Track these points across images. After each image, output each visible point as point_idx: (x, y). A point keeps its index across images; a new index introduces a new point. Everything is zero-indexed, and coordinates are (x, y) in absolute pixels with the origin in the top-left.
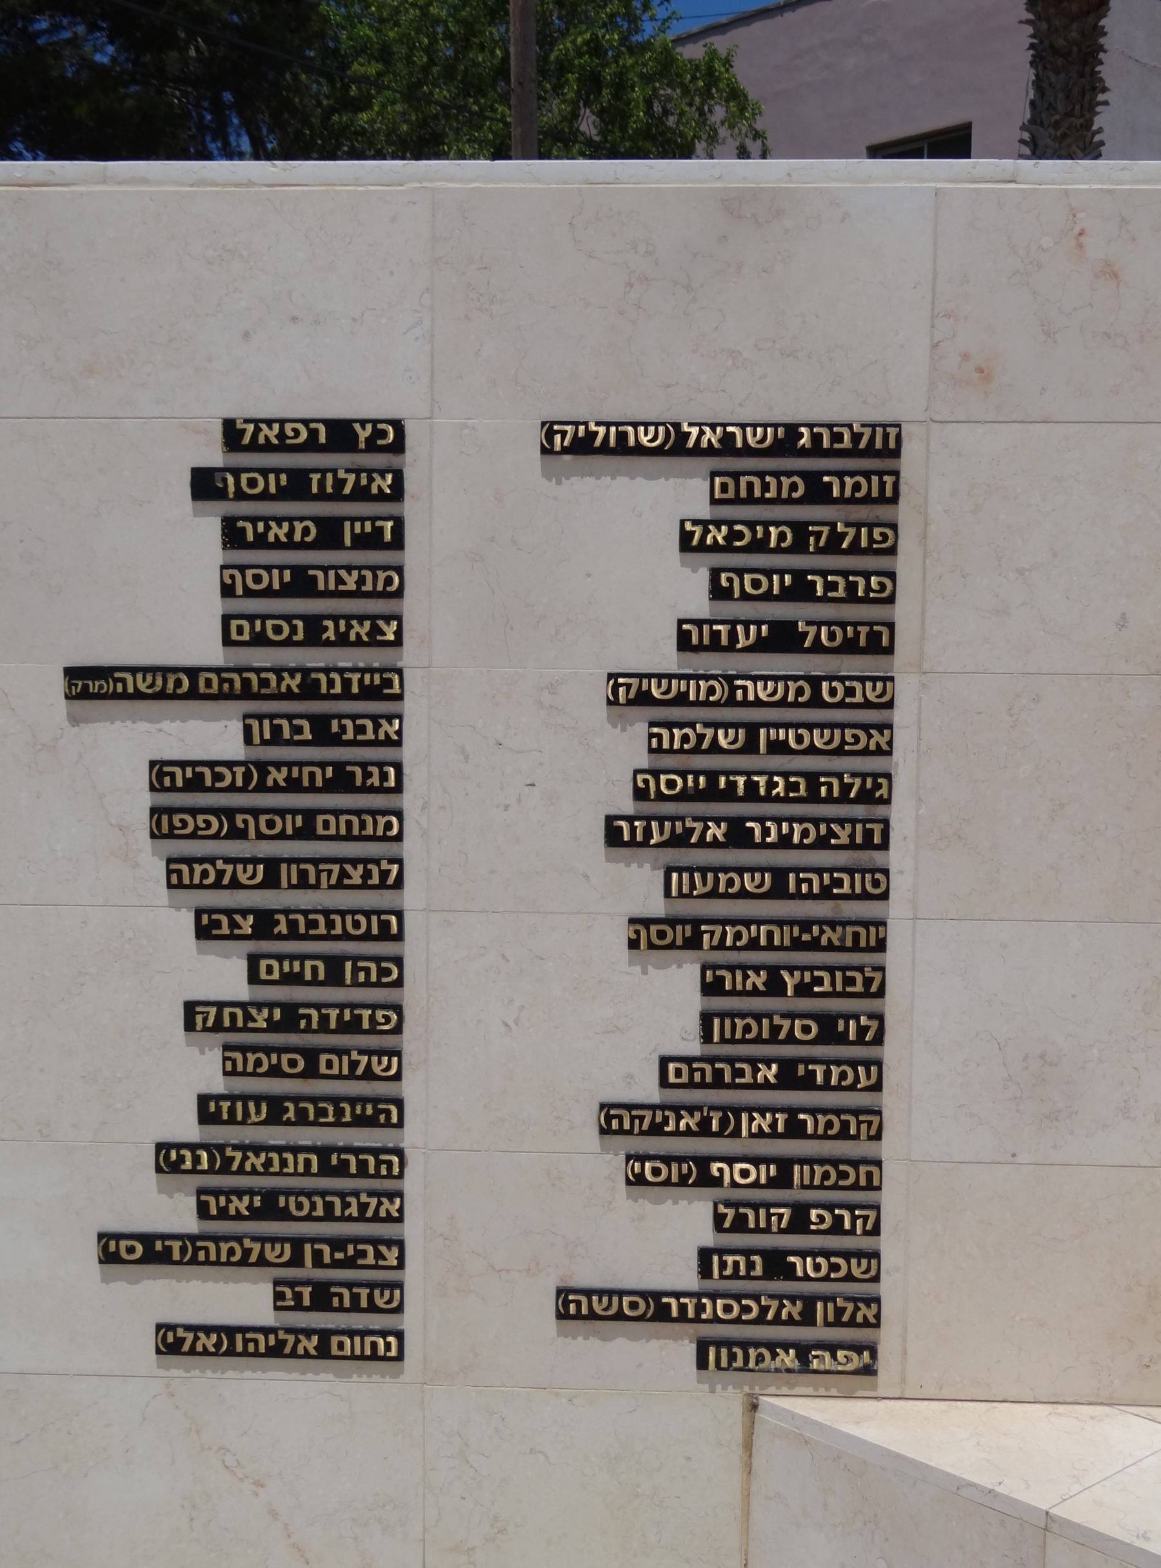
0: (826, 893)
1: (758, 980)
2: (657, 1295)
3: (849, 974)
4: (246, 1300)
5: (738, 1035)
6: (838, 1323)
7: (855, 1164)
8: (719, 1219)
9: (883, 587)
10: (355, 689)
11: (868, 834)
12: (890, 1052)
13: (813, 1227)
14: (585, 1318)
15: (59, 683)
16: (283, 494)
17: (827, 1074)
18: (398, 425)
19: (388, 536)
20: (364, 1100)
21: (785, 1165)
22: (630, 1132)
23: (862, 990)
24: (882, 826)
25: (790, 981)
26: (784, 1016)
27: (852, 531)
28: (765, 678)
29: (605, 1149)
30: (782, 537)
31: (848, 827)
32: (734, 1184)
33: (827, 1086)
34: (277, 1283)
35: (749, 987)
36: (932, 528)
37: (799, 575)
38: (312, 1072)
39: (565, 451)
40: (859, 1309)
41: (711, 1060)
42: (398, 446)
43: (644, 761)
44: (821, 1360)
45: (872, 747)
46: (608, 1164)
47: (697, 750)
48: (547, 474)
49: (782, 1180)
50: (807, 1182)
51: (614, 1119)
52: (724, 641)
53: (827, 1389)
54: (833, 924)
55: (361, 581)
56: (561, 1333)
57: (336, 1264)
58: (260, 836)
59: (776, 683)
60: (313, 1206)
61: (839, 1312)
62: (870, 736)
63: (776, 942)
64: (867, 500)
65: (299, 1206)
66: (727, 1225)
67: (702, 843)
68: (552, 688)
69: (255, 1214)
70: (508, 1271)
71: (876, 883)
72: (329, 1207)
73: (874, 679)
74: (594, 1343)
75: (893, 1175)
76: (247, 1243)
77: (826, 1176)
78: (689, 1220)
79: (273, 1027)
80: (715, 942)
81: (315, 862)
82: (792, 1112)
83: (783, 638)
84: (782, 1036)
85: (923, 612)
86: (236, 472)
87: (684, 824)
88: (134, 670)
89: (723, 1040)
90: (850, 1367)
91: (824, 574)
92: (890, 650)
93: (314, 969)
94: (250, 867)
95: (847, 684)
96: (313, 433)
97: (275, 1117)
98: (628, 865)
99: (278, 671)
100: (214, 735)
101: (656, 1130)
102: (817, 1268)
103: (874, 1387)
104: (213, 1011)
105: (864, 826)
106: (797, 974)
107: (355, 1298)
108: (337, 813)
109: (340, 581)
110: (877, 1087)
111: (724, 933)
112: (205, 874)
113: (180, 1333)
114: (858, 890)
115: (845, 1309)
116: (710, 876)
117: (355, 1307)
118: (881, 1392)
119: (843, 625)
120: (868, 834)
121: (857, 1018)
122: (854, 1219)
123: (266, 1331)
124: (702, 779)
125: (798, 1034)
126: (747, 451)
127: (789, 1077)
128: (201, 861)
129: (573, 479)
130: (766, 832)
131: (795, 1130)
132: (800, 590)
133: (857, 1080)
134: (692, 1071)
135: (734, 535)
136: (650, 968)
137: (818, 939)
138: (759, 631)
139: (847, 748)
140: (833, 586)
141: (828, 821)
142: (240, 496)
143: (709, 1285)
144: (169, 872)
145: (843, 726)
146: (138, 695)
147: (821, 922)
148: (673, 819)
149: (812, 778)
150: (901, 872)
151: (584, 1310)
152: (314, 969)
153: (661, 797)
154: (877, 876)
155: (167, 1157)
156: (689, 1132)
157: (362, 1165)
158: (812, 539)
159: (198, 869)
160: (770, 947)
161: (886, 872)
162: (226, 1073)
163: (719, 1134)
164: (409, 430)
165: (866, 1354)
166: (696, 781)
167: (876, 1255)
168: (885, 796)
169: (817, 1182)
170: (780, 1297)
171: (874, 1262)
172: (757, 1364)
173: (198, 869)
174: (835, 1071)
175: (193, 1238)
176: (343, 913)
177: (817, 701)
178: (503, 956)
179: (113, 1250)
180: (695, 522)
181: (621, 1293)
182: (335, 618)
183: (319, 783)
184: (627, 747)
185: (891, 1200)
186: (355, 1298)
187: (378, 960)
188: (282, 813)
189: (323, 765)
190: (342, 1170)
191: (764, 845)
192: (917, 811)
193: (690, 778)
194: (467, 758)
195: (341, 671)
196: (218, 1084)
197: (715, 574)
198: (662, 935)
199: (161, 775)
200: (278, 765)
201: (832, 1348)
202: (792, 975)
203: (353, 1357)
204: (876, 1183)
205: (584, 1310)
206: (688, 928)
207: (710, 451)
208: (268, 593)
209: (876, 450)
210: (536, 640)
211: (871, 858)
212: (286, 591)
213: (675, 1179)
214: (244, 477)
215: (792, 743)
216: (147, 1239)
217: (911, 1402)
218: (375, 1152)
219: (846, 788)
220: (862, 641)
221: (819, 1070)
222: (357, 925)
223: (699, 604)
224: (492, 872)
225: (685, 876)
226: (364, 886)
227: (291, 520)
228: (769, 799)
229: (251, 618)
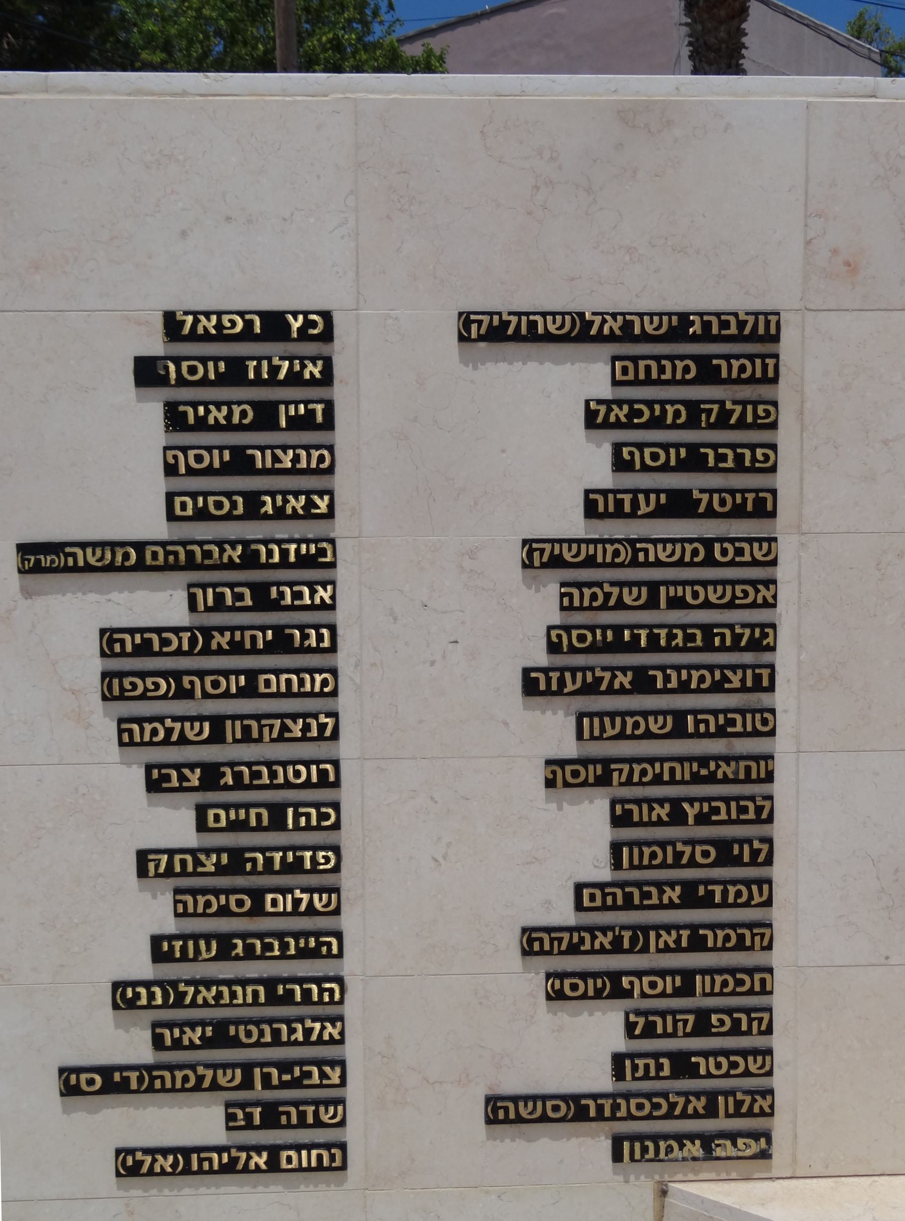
0: (721, 732)
1: (663, 812)
2: (575, 1098)
3: (742, 803)
4: (199, 1122)
5: (646, 862)
6: (738, 1114)
7: (750, 972)
8: (630, 1028)
9: (767, 458)
10: (292, 559)
11: (758, 678)
12: (778, 872)
13: (714, 1030)
14: (512, 1122)
15: (12, 559)
16: (222, 380)
17: (725, 893)
18: (327, 316)
19: (319, 418)
20: (307, 934)
21: (688, 975)
22: (550, 953)
23: (754, 817)
24: (769, 671)
25: (691, 812)
26: (685, 843)
27: (738, 409)
28: (664, 541)
29: (526, 970)
30: (677, 414)
31: (740, 673)
32: (644, 995)
33: (724, 904)
34: (228, 1105)
35: (654, 818)
36: (808, 405)
37: (693, 448)
38: (258, 910)
39: (481, 338)
40: (756, 1101)
41: (622, 885)
42: (327, 336)
43: (556, 618)
44: (725, 1148)
45: (760, 601)
46: (530, 981)
47: (604, 607)
48: (464, 361)
49: (687, 990)
50: (708, 990)
51: (534, 941)
52: (627, 508)
53: (728, 1173)
54: (727, 759)
55: (296, 459)
56: (491, 1137)
57: (283, 1085)
58: (206, 695)
59: (674, 545)
60: (261, 1034)
61: (739, 1104)
62: (757, 591)
63: (678, 777)
64: (752, 380)
65: (249, 1034)
66: (637, 1032)
67: (610, 691)
68: (472, 554)
69: (207, 1043)
70: (440, 1083)
71: (765, 722)
72: (276, 1033)
73: (760, 540)
74: (520, 1145)
75: (781, 981)
76: (201, 1070)
77: (725, 984)
79: (221, 870)
80: (624, 779)
81: (258, 717)
82: (694, 928)
83: (679, 505)
84: (684, 861)
85: (802, 479)
86: (177, 360)
87: (593, 674)
88: (83, 545)
89: (632, 867)
90: (748, 1152)
91: (715, 446)
92: (773, 514)
93: (259, 816)
94: (197, 725)
95: (737, 545)
96: (249, 324)
97: (225, 953)
98: (543, 712)
99: (220, 544)
100: (161, 604)
101: (574, 949)
102: (718, 1066)
103: (769, 1169)
104: (165, 858)
105: (754, 671)
106: (697, 805)
107: (302, 1115)
108: (277, 672)
109: (276, 459)
110: (768, 903)
111: (631, 771)
112: (154, 732)
113: (139, 1156)
114: (749, 728)
115: (744, 1101)
116: (618, 720)
117: (302, 1123)
118: (775, 1173)
119: (732, 492)
120: (758, 678)
121: (750, 842)
122: (750, 1021)
123: (219, 1150)
124: (609, 634)
125: (699, 859)
126: (645, 337)
127: (692, 896)
128: (150, 720)
129: (488, 364)
130: (667, 679)
131: (698, 944)
132: (694, 461)
133: (751, 896)
134: (604, 895)
135: (634, 413)
136: (565, 805)
137: (715, 772)
138: (658, 499)
139: (737, 602)
140: (724, 458)
141: (722, 667)
142: (182, 382)
143: (623, 1086)
144: (120, 732)
145: (734, 583)
146: (88, 568)
147: (716, 758)
148: (583, 669)
149: (707, 629)
150: (786, 711)
151: (512, 1116)
152: (259, 816)
153: (573, 650)
154: (766, 715)
155: (123, 994)
156: (603, 951)
157: (307, 993)
158: (704, 416)
159: (148, 727)
160: (673, 781)
161: (773, 711)
162: (177, 915)
163: (630, 951)
164: (337, 319)
165: (763, 1140)
166: (604, 635)
167: (769, 1052)
168: (772, 644)
169: (717, 989)
170: (686, 1094)
171: (768, 1058)
172: (666, 1155)
173: (148, 727)
174: (732, 890)
175: (149, 1068)
176: (284, 764)
177: (710, 561)
178: (432, 798)
179: (72, 1083)
180: (599, 402)
181: (544, 1098)
182: (273, 494)
183: (260, 645)
184: (540, 606)
185: (781, 1002)
186: (302, 1115)
187: (317, 806)
188: (226, 674)
189: (263, 629)
190: (288, 999)
191: (666, 691)
192: (799, 657)
193: (598, 632)
194: (395, 619)
195: (279, 542)
196: (170, 925)
197: (617, 448)
198: (575, 774)
199: (111, 642)
200: (221, 630)
201: (733, 1137)
202: (692, 806)
203: (300, 1169)
204: (768, 988)
205: (512, 1116)
206: (599, 767)
207: (612, 338)
208: (209, 471)
209: (758, 335)
210: (454, 511)
211: (760, 700)
212: (226, 470)
213: (591, 993)
214: (185, 365)
215: (689, 599)
216: (106, 1071)
217: (802, 1180)
218: (318, 981)
219: (737, 638)
220: (750, 507)
221: (718, 889)
222: (297, 774)
223: (602, 475)
224: (420, 722)
225: (596, 721)
226: (304, 739)
227: (229, 404)
228: (669, 649)
229: (194, 495)
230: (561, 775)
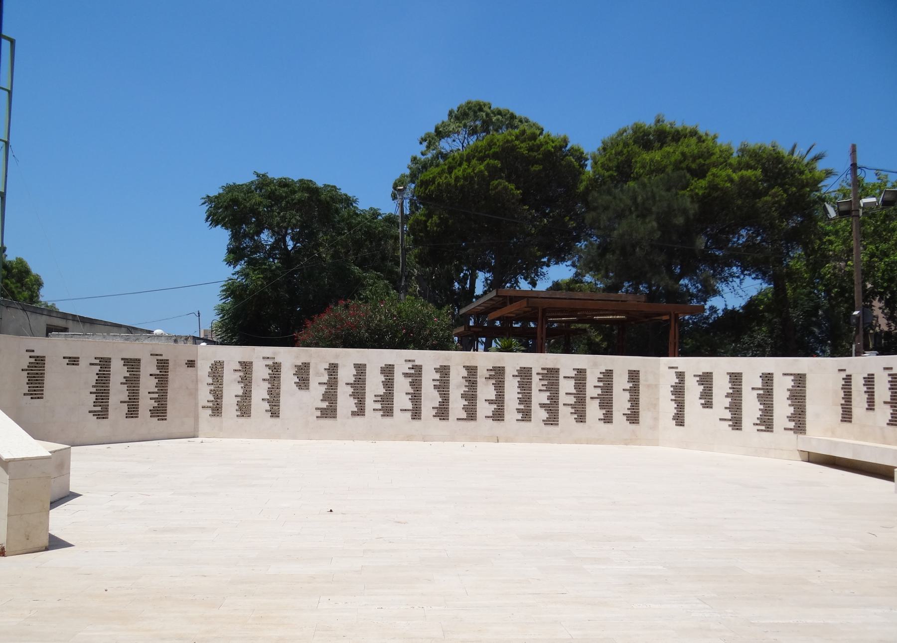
4: (763, 428)
100: (761, 392)
184: (788, 393)
230: (790, 405)
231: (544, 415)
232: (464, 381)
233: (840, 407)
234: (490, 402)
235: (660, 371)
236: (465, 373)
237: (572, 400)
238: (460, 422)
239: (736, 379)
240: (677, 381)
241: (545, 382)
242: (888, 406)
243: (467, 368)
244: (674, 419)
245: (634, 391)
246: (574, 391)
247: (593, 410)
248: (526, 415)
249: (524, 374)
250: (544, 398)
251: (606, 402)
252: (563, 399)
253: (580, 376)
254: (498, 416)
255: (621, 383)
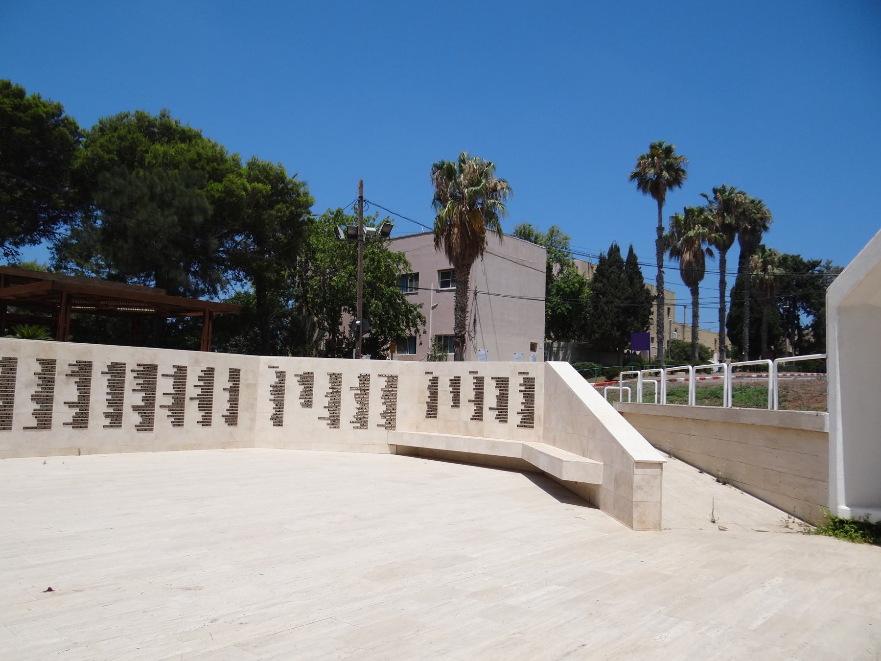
4: (359, 425)
78: (385, 420)
100: (358, 392)
230: (383, 404)
231: (137, 419)
232: (36, 378)
233: (426, 405)
234: (71, 405)
235: (260, 369)
236: (38, 368)
237: (169, 401)
238: (28, 432)
239: (335, 379)
240: (277, 380)
241: (141, 381)
242: (473, 404)
243: (42, 362)
244: (272, 419)
245: (234, 391)
246: (173, 391)
247: (192, 412)
248: (115, 420)
249: (116, 371)
250: (137, 399)
251: (205, 404)
252: (161, 400)
253: (180, 373)
254: (80, 422)
255: (221, 382)
